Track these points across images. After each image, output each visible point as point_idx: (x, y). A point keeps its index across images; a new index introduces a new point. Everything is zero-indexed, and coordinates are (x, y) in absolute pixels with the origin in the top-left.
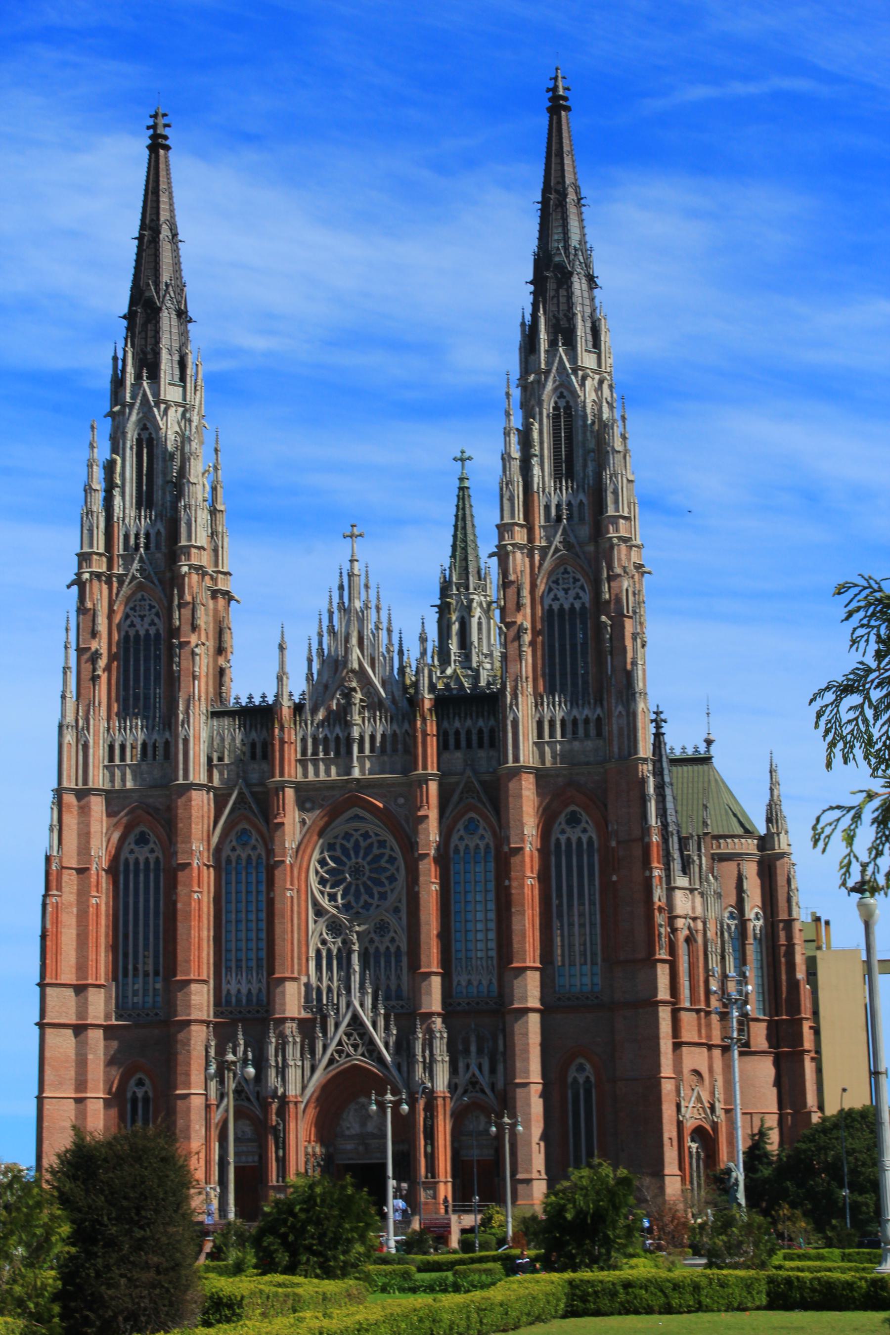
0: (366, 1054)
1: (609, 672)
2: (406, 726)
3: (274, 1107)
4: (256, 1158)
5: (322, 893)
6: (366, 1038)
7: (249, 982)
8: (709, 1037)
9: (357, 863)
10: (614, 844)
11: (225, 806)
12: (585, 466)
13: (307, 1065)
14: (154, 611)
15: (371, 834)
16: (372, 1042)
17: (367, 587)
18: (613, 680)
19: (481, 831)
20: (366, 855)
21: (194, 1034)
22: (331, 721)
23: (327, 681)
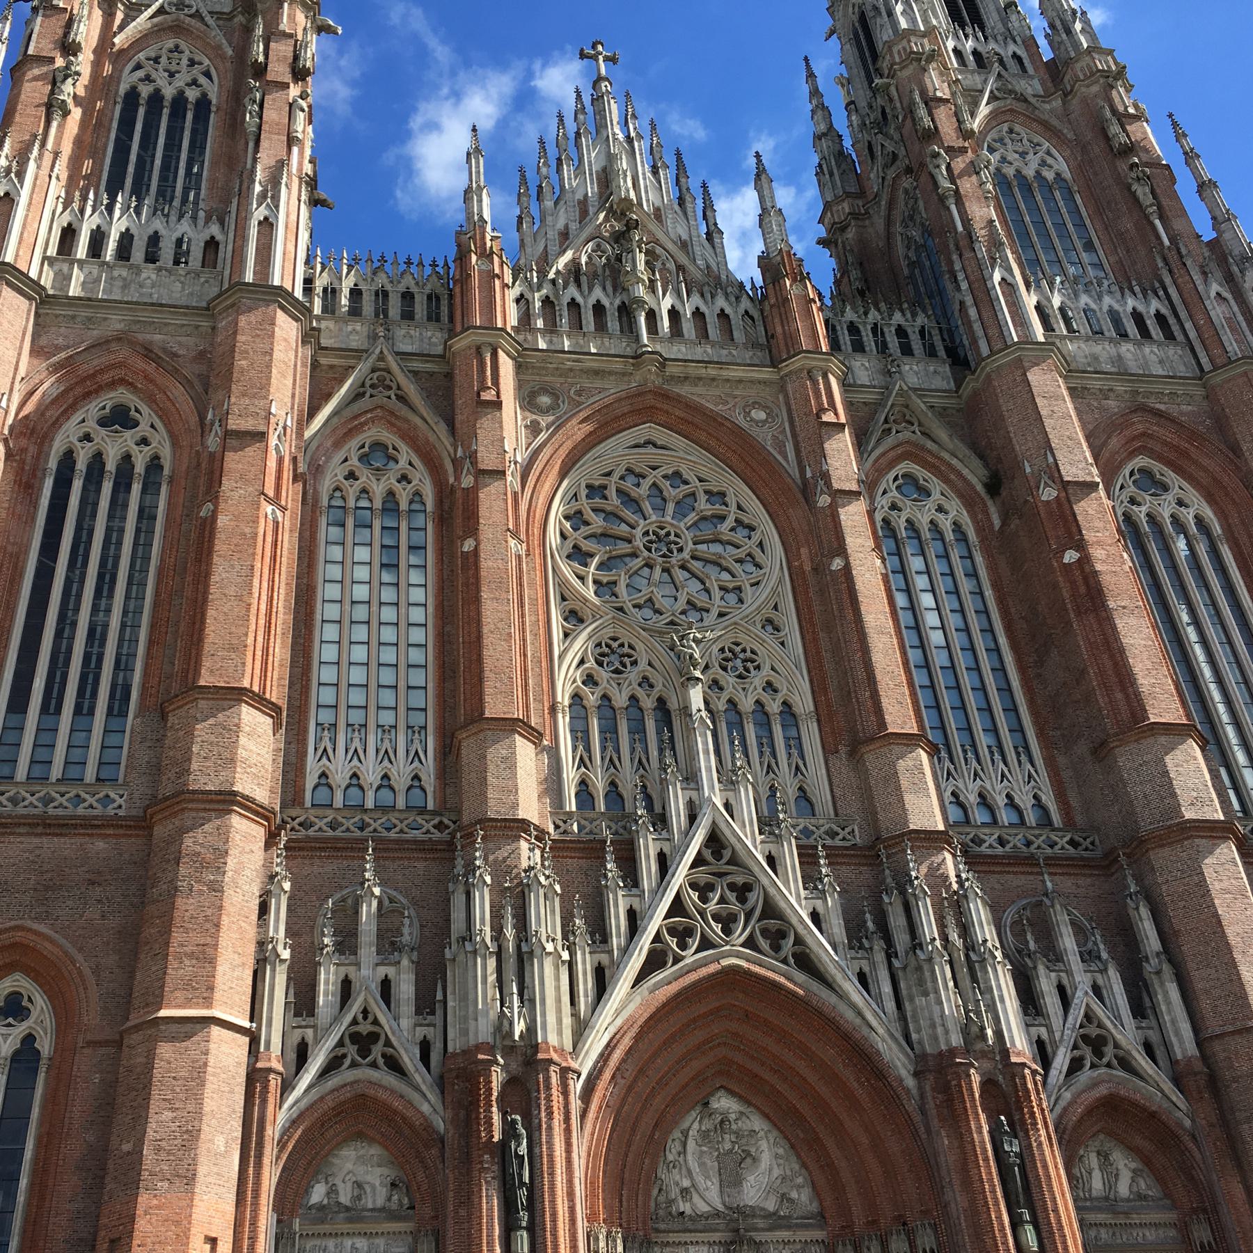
0: (764, 944)
1: (1166, 242)
2: (745, 304)
3: (497, 1077)
6: (753, 897)
7: (387, 756)
11: (328, 396)
13: (585, 964)
16: (771, 910)
18: (1184, 251)
19: (936, 495)
20: (681, 512)
21: (236, 838)
22: (584, 279)
23: (566, 226)
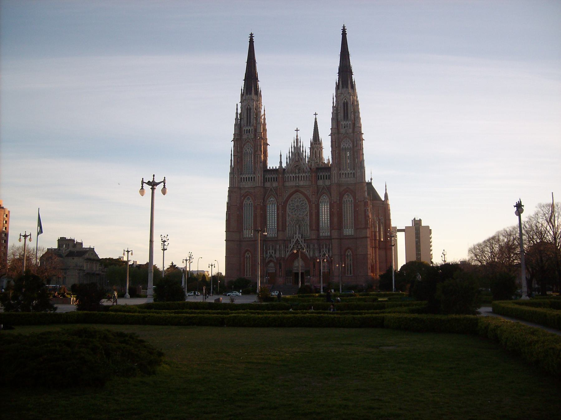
2: (309, 174)
4: (275, 271)
5: (289, 212)
6: (300, 245)
8: (372, 246)
9: (298, 205)
10: (357, 202)
12: (351, 115)
14: (251, 147)
15: (301, 198)
17: (300, 142)
